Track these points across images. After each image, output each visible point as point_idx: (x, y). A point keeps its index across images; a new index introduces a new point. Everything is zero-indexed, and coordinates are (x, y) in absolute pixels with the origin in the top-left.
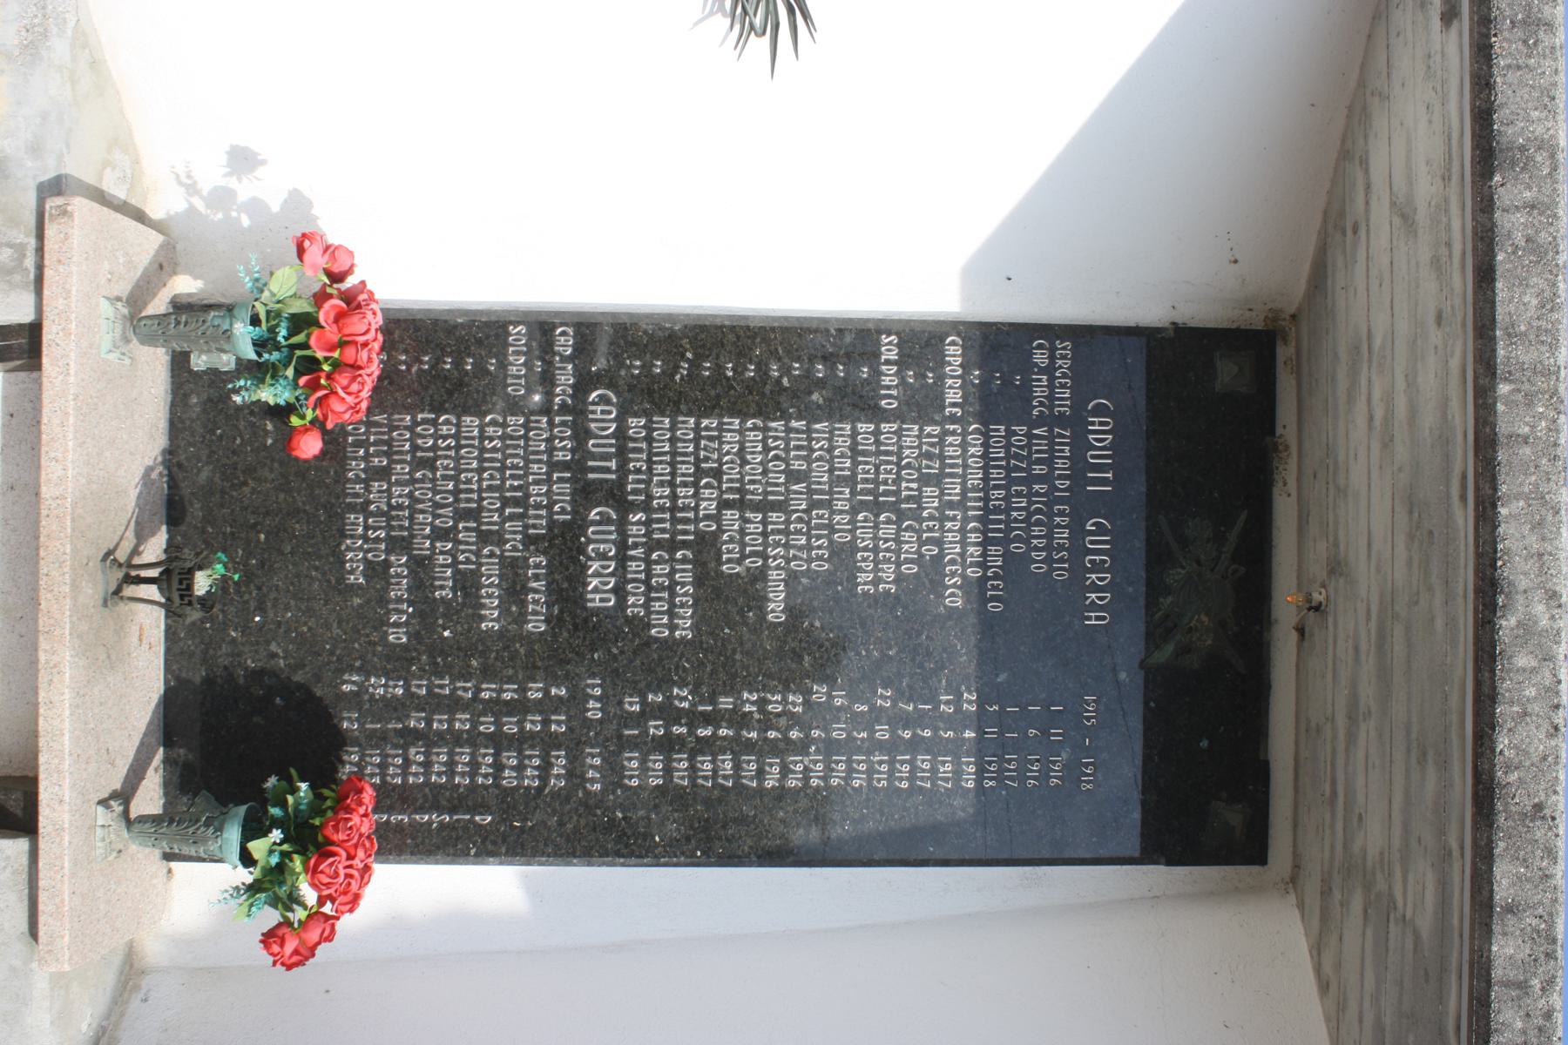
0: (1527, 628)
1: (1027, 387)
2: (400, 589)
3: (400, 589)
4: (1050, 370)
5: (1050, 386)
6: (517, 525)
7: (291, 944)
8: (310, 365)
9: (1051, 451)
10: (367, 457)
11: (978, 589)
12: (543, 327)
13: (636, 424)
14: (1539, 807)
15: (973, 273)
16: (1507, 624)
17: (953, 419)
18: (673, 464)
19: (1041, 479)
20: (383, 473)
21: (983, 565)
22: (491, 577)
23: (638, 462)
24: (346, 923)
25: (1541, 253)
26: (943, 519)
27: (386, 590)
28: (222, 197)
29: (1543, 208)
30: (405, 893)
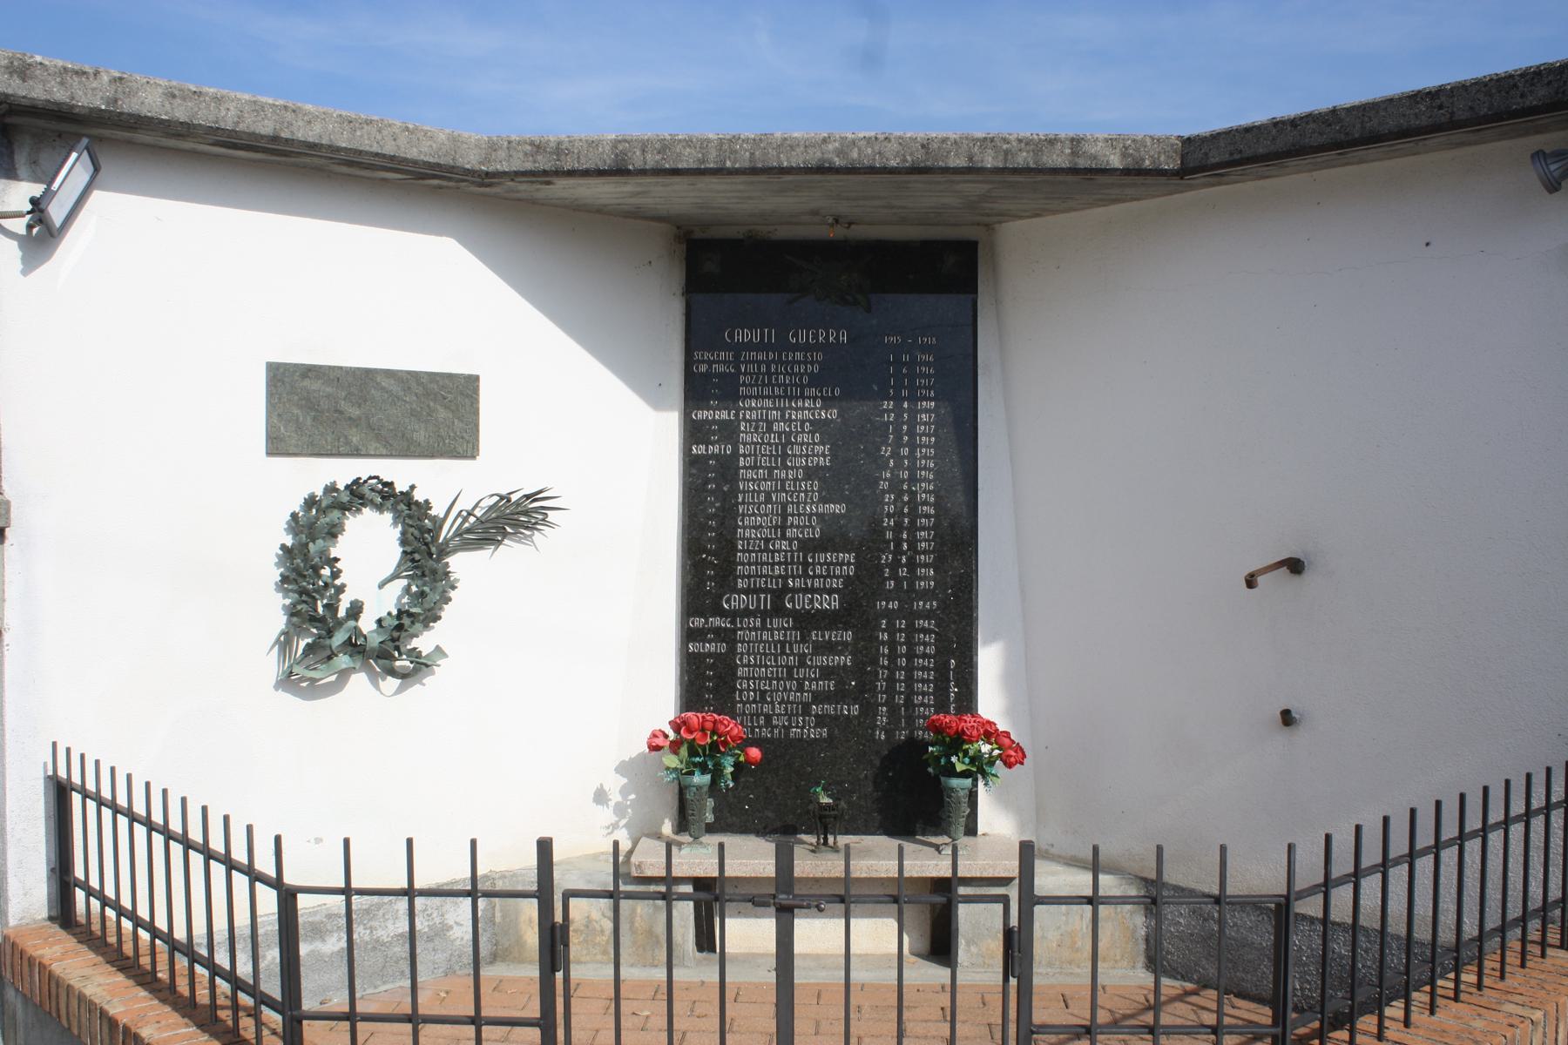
0: (840, 152)
1: (721, 375)
2: (830, 709)
3: (830, 709)
4: (710, 363)
5: (717, 363)
6: (795, 647)
7: (1012, 755)
8: (714, 747)
9: (753, 362)
10: (760, 727)
11: (828, 402)
12: (688, 635)
13: (740, 584)
14: (923, 146)
15: (657, 404)
16: (838, 162)
17: (737, 415)
18: (762, 564)
19: (768, 368)
20: (768, 718)
21: (815, 399)
22: (823, 660)
23: (761, 583)
24: (1001, 728)
25: (665, 146)
26: (790, 420)
27: (830, 716)
28: (619, 810)
29: (644, 145)
30: (991, 703)
